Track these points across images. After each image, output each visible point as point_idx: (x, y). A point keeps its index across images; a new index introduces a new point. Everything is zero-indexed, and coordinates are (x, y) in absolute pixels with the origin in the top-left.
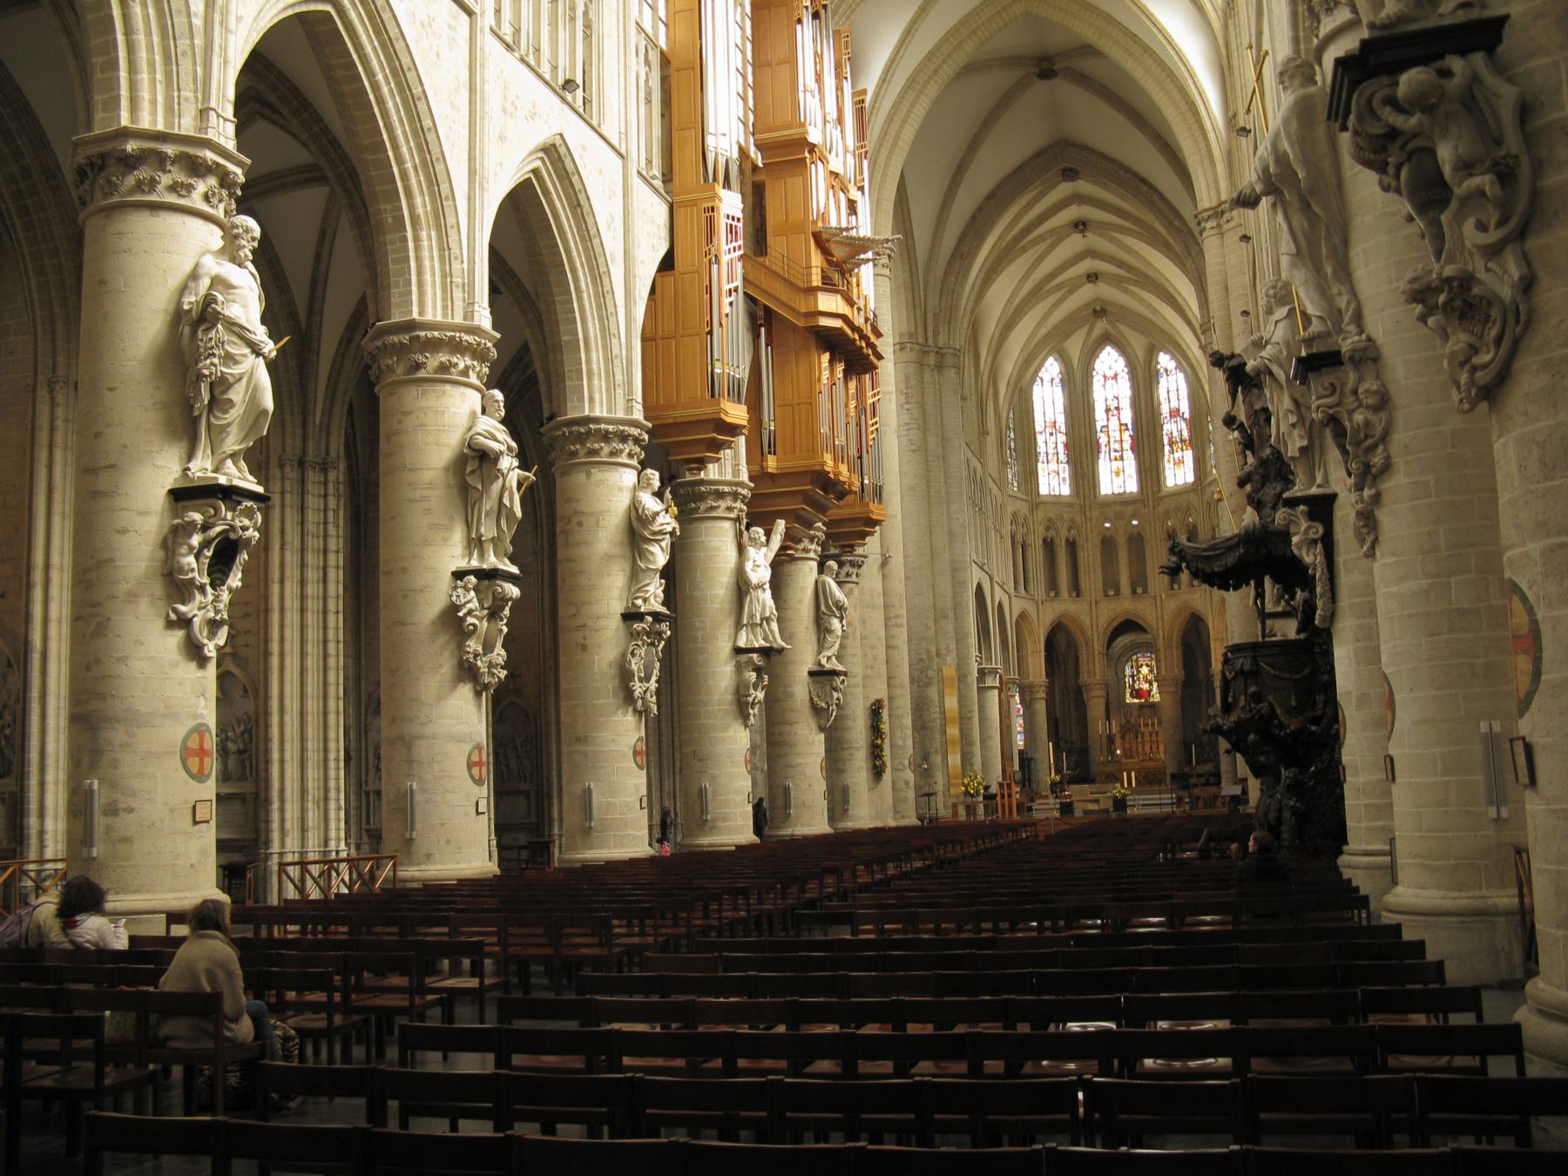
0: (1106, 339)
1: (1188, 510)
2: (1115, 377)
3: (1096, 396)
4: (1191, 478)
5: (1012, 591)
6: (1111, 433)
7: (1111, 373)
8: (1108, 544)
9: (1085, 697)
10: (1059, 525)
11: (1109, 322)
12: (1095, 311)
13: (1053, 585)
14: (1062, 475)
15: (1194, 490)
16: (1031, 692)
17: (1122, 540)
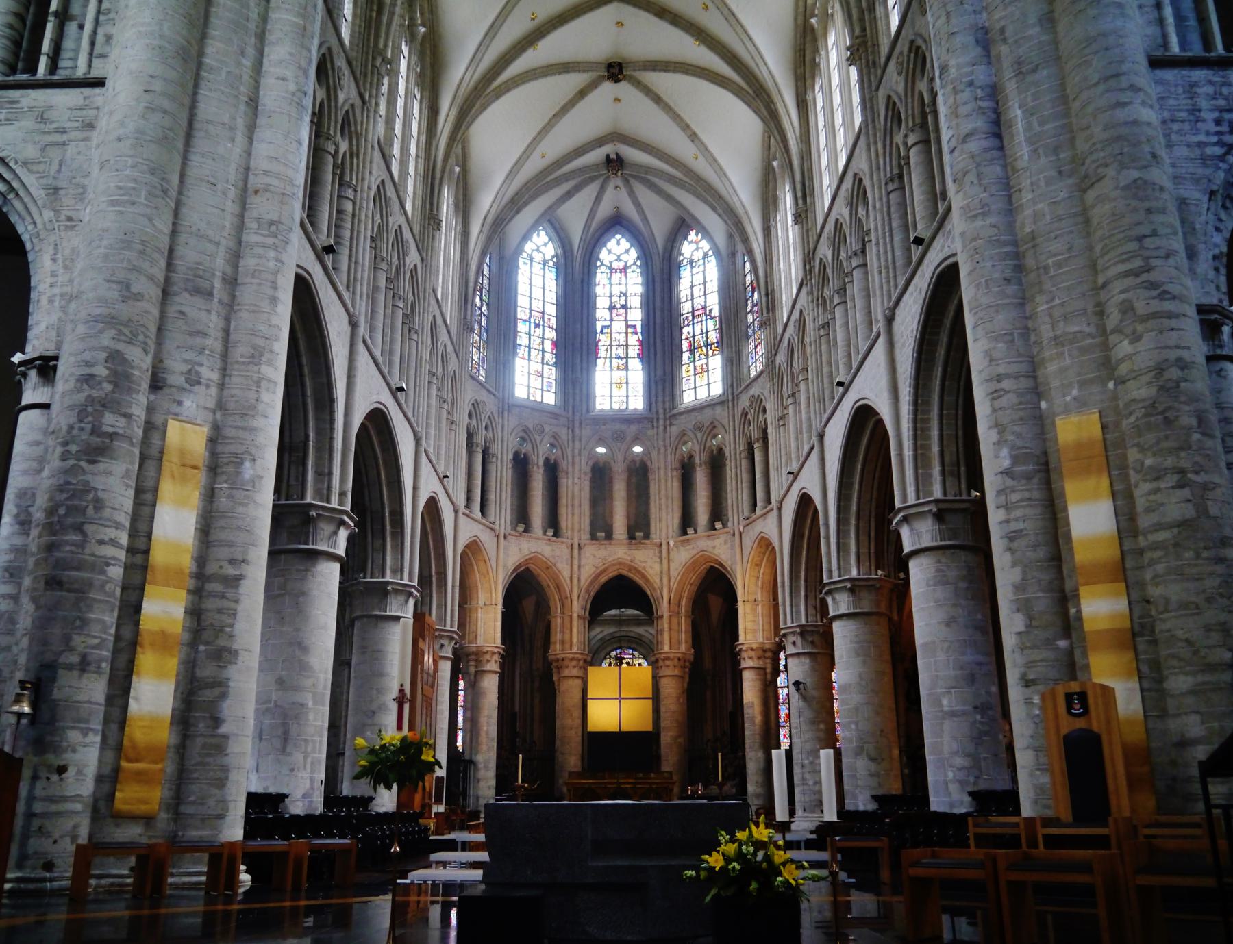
0: (616, 223)
1: (712, 430)
2: (624, 270)
3: (599, 290)
4: (717, 389)
5: (461, 500)
6: (613, 336)
7: (621, 265)
8: (600, 475)
9: (555, 678)
10: (538, 438)
11: (626, 181)
12: (608, 159)
13: (522, 517)
14: (545, 380)
15: (722, 403)
16: (478, 662)
17: (619, 468)
